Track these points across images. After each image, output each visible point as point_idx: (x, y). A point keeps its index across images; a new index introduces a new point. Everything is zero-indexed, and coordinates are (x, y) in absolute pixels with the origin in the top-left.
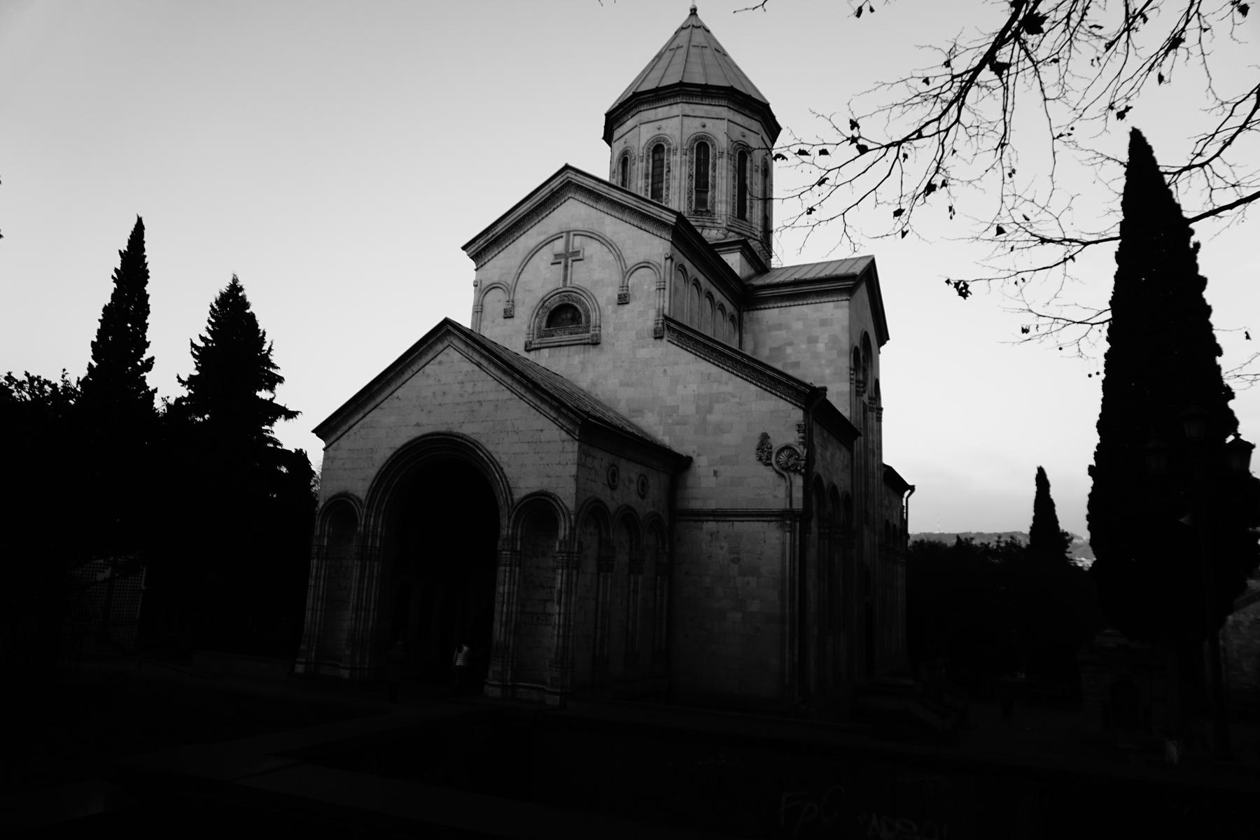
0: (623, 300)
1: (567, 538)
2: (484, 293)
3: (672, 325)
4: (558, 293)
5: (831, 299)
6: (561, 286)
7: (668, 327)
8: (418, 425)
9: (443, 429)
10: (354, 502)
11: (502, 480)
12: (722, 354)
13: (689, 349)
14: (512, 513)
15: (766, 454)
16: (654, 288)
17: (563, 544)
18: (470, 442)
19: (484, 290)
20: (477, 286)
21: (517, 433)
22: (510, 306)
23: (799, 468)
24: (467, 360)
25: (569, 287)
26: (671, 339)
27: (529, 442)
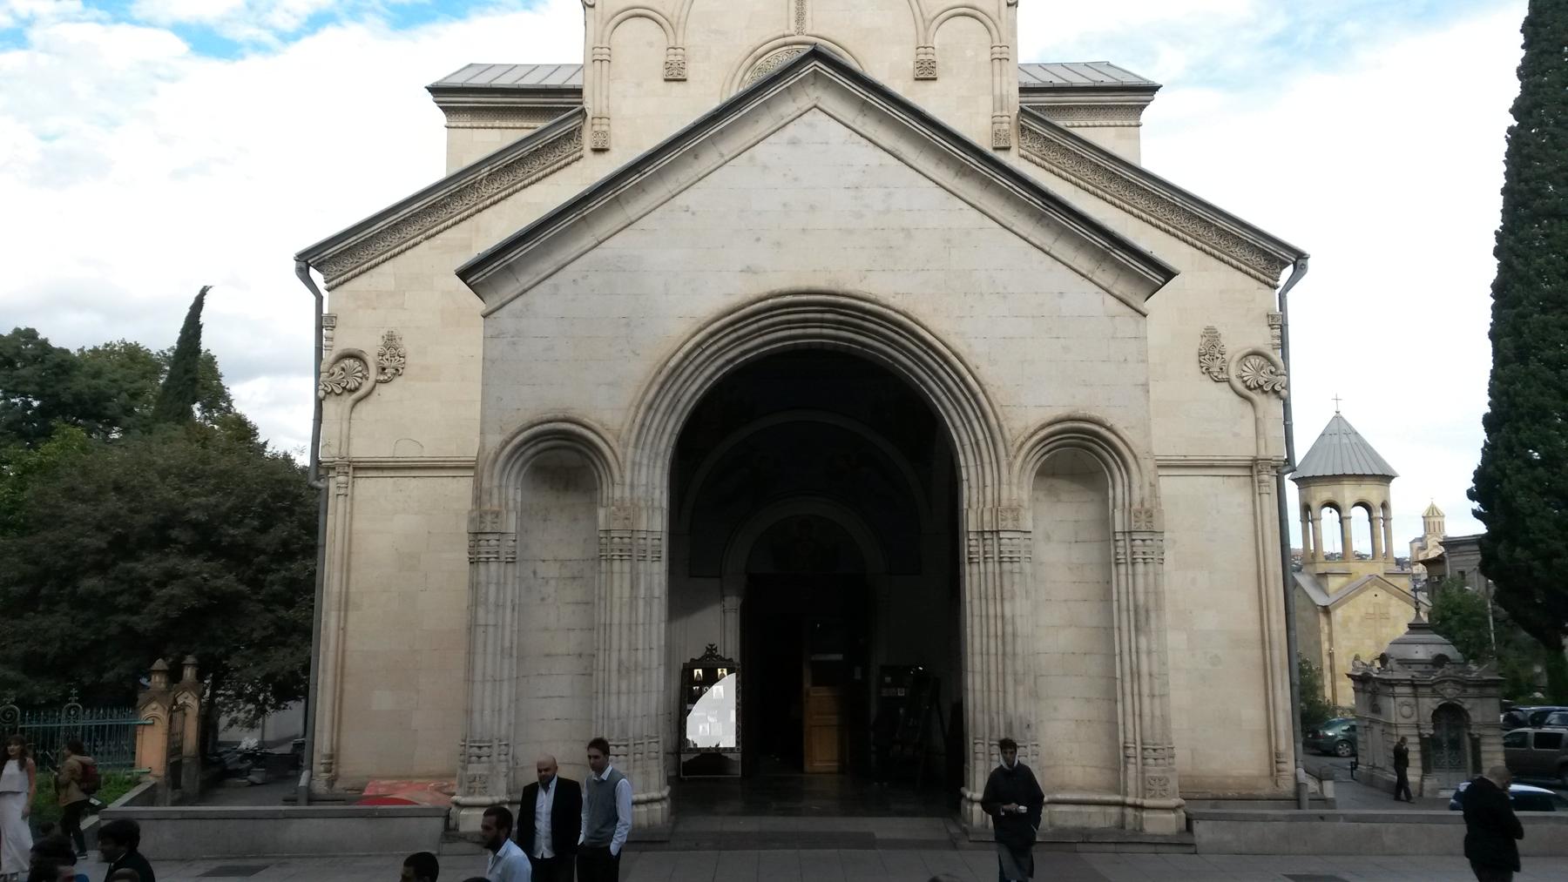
0: (926, 73)
1: (1147, 505)
2: (613, 23)
3: (1036, 127)
4: (785, 45)
5: (1112, 123)
6: (793, 30)
7: (1023, 130)
8: (748, 270)
9: (821, 283)
10: (602, 438)
11: (984, 392)
12: (1129, 184)
13: (1064, 174)
14: (1015, 457)
15: (1218, 362)
16: (987, 57)
17: (1143, 517)
18: (897, 312)
19: (613, 17)
20: (593, 6)
21: (1005, 297)
22: (679, 58)
23: (1277, 388)
24: (864, 141)
25: (807, 35)
26: (1022, 152)
27: (1033, 317)
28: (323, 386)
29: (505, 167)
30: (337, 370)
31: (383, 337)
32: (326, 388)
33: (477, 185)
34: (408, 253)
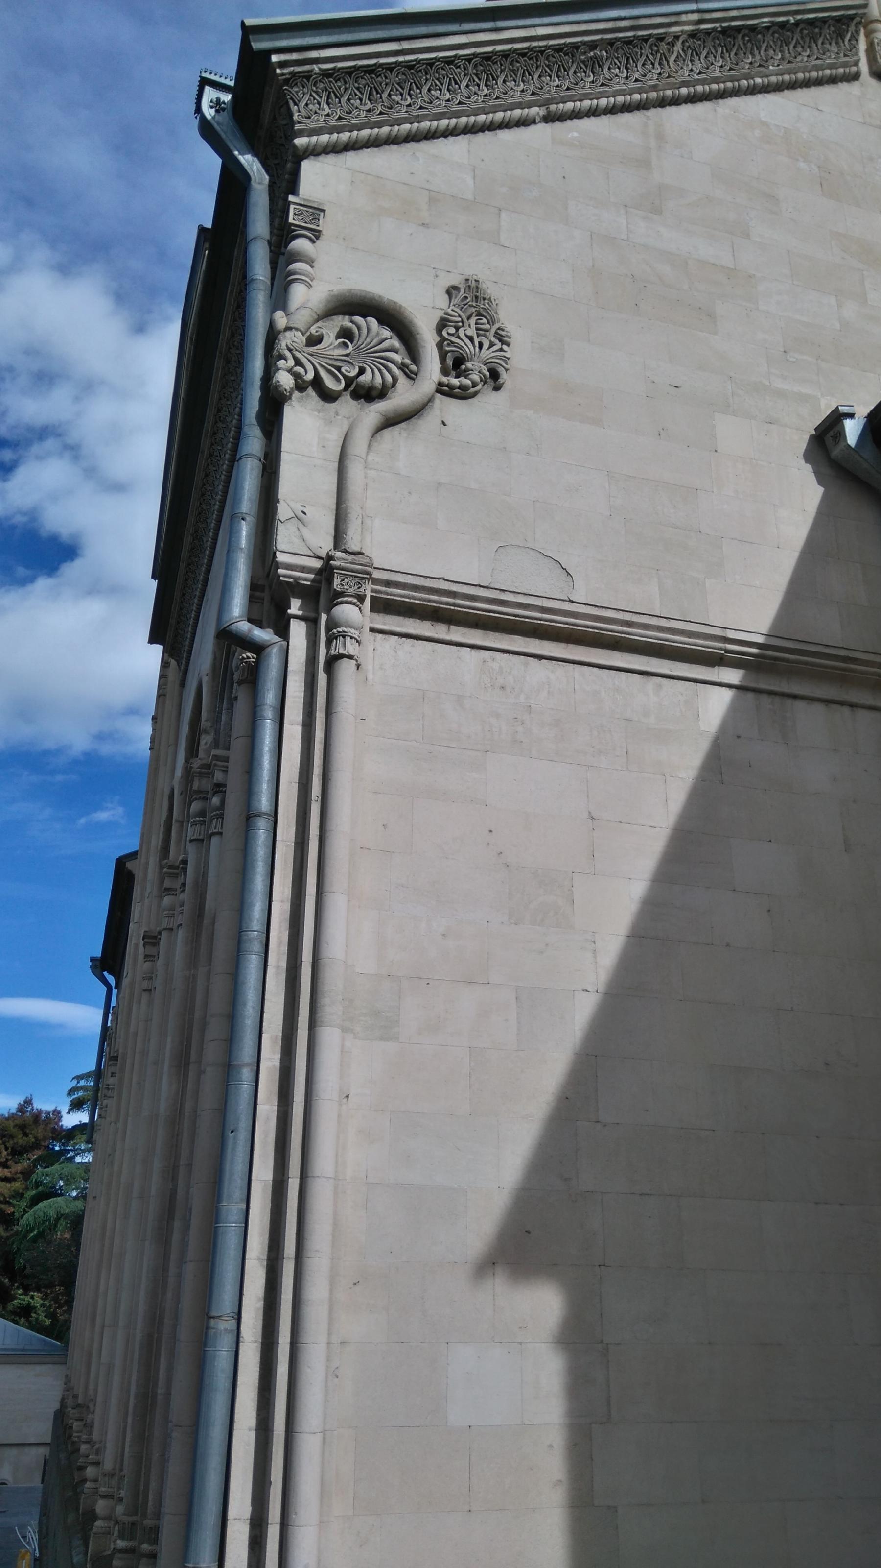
28: (291, 362)
29: (725, 31)
30: (330, 330)
31: (451, 291)
32: (299, 369)
33: (663, 46)
34: (504, 135)
